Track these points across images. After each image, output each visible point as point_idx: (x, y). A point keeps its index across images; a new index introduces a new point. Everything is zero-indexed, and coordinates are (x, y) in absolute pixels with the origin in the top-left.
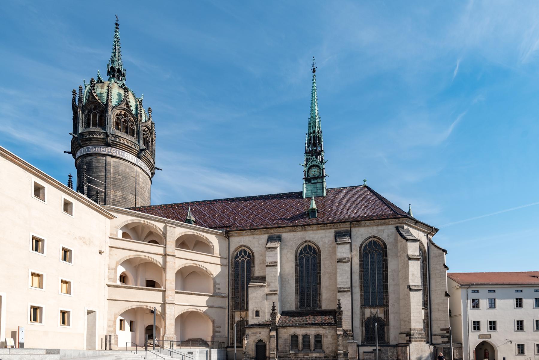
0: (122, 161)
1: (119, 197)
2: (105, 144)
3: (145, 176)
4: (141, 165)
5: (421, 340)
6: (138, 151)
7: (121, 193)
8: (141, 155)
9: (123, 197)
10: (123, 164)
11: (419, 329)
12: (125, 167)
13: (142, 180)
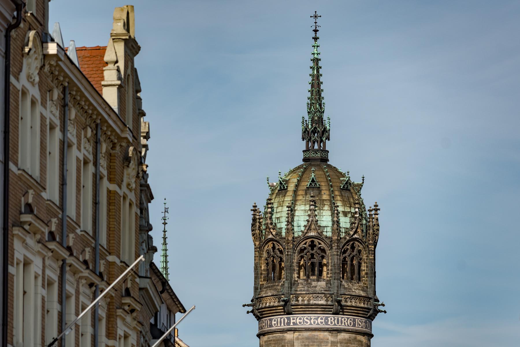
3: (308, 338)
4: (296, 324)
8: (289, 308)
10: (271, 340)
12: (274, 344)
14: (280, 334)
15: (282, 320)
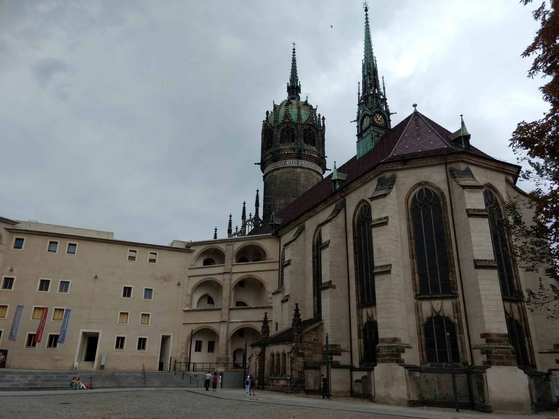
0: (285, 170)
1: (283, 204)
2: (273, 161)
4: (302, 165)
5: (391, 360)
6: (296, 153)
7: (283, 200)
9: (285, 204)
11: (391, 339)
13: (304, 178)
14: (291, 169)
15: (294, 162)
